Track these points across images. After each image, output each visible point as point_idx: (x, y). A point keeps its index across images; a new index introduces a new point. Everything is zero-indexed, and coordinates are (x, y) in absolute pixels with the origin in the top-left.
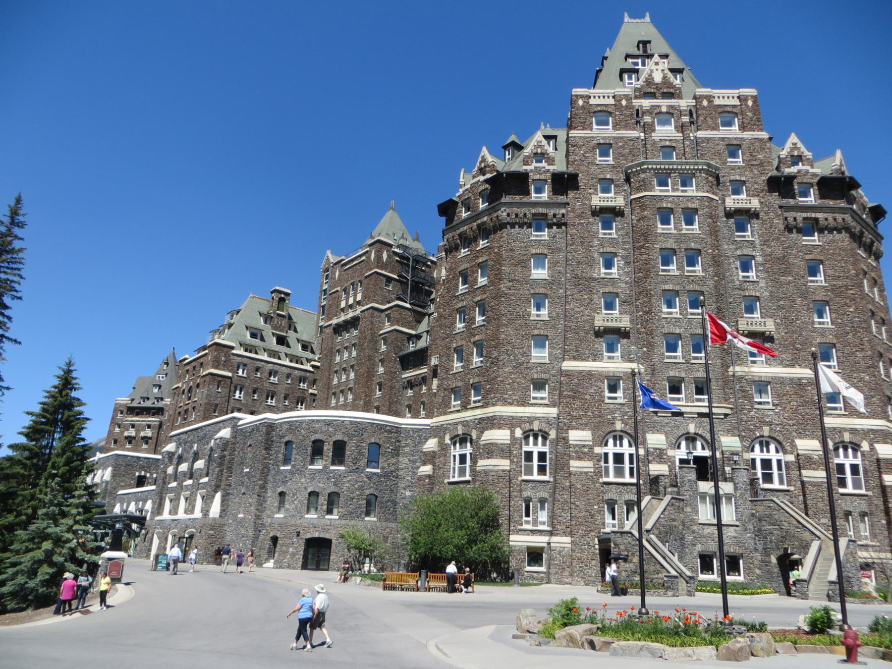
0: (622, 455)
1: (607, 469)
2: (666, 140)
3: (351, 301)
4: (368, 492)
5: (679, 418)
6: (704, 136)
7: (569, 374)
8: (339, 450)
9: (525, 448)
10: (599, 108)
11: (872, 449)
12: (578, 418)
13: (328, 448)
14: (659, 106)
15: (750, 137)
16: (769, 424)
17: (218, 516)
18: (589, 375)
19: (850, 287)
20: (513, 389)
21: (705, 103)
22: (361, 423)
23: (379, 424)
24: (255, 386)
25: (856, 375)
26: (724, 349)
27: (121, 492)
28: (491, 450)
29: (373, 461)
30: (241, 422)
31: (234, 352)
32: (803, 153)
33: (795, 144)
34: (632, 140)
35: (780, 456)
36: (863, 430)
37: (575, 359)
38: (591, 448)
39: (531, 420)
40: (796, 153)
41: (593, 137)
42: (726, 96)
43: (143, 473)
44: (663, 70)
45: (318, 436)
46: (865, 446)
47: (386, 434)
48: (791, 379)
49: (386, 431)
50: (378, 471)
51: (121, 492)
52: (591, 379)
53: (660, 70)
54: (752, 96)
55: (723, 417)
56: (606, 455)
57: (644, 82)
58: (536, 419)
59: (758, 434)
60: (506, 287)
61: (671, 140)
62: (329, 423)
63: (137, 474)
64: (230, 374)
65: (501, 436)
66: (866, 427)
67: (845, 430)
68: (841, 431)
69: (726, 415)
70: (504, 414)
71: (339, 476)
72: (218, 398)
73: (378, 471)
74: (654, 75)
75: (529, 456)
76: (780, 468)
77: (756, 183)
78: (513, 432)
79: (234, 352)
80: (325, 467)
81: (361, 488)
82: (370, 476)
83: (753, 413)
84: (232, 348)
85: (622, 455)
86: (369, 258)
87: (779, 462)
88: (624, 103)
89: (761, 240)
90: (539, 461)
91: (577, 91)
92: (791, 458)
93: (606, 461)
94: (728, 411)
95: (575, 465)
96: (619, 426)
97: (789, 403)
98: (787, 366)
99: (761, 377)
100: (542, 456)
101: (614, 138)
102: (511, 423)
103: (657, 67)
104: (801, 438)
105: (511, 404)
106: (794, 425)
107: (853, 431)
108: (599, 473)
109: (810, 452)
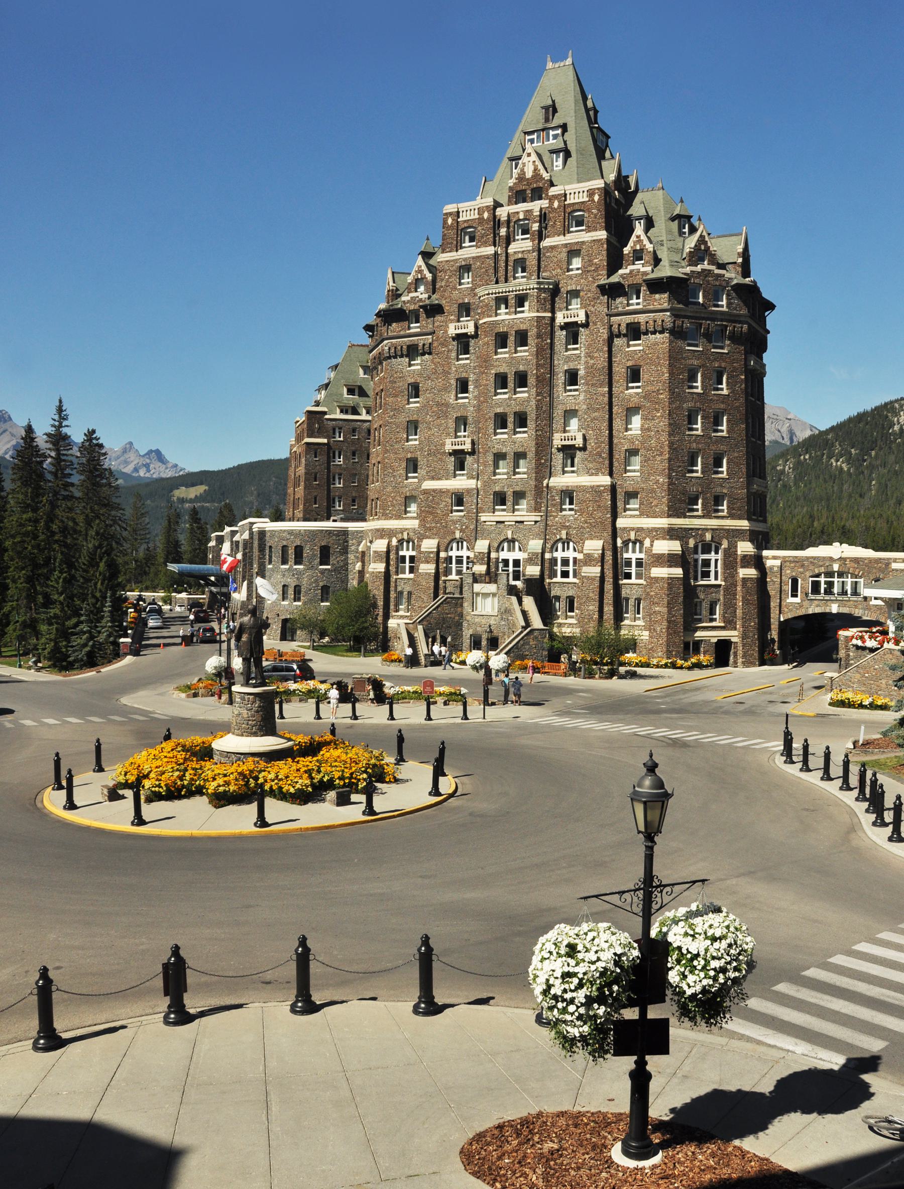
2: (519, 252)
4: (321, 584)
5: (501, 526)
6: (549, 244)
7: (426, 492)
8: (299, 551)
10: (466, 225)
11: (652, 545)
12: (430, 529)
13: (291, 551)
14: (518, 213)
15: (590, 239)
16: (568, 528)
17: (245, 599)
19: (661, 392)
20: (393, 506)
21: (556, 204)
22: (313, 531)
23: (327, 530)
24: (353, 448)
25: (652, 477)
26: (541, 464)
29: (324, 560)
30: (255, 526)
31: (327, 417)
32: (645, 245)
34: (488, 258)
35: (576, 555)
36: (648, 529)
37: (433, 478)
38: (438, 553)
39: (402, 531)
40: (638, 247)
41: (456, 260)
42: (572, 192)
44: (534, 162)
45: (285, 543)
46: (647, 542)
47: (334, 537)
48: (592, 487)
49: (334, 535)
50: (329, 567)
52: (441, 496)
53: (531, 163)
54: (598, 189)
55: (533, 523)
57: (516, 179)
59: (558, 537)
60: (389, 417)
61: (523, 251)
62: (291, 532)
64: (325, 441)
66: (650, 526)
67: (633, 529)
69: (536, 522)
70: (385, 527)
71: (300, 573)
72: (316, 466)
73: (329, 567)
74: (526, 170)
75: (404, 557)
77: (589, 291)
79: (327, 417)
80: (291, 566)
81: (316, 581)
82: (323, 572)
83: (557, 519)
84: (325, 413)
87: (575, 559)
89: (587, 353)
90: (410, 563)
91: (450, 208)
92: (580, 556)
94: (538, 519)
96: (458, 535)
97: (587, 508)
98: (592, 474)
99: (568, 487)
101: (473, 258)
103: (529, 159)
104: (592, 539)
106: (588, 527)
107: (639, 530)
109: (593, 552)
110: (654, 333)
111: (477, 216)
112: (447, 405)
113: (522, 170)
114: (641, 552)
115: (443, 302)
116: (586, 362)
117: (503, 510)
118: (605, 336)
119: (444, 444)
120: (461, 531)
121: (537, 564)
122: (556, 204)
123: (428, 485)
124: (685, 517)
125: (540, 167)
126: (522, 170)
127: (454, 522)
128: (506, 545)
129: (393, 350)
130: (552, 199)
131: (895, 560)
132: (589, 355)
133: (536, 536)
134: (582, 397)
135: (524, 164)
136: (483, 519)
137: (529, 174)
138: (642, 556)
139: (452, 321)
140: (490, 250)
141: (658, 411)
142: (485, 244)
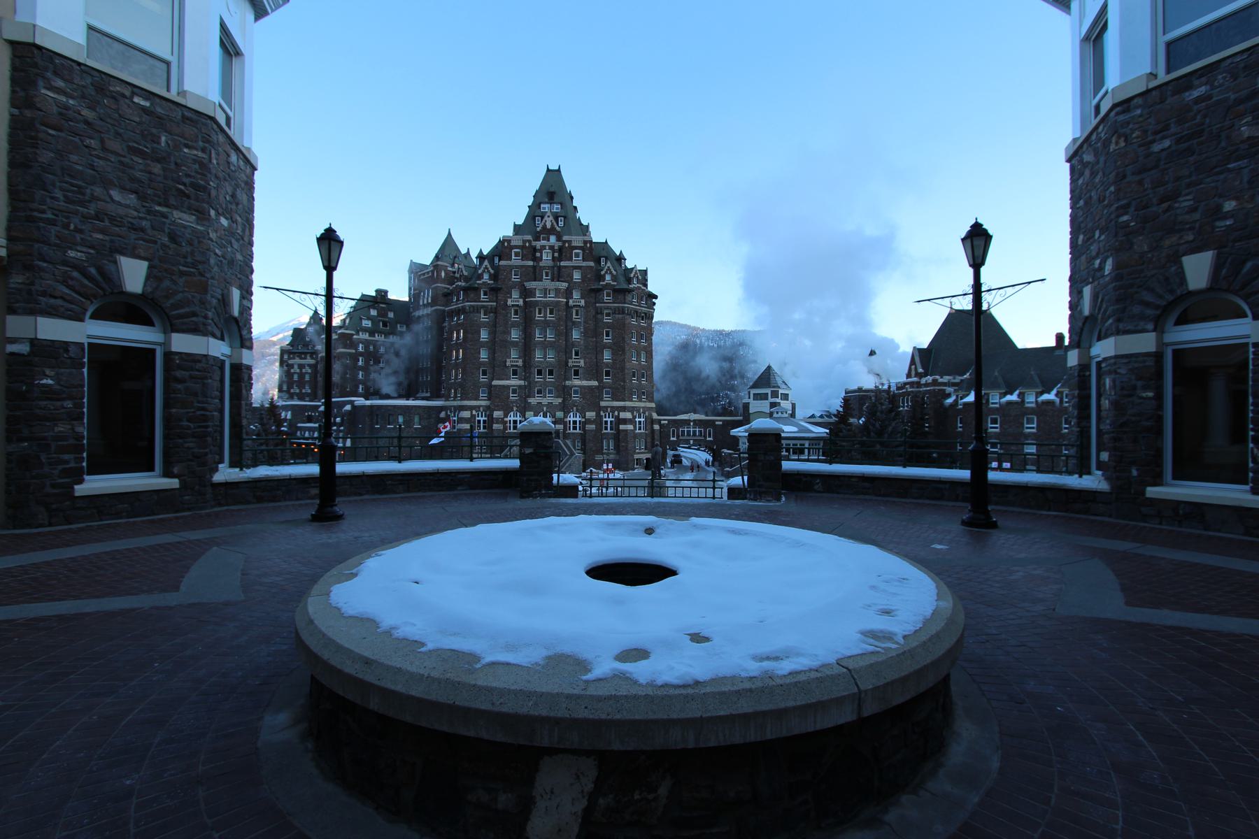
0: (516, 421)
1: (510, 427)
3: (425, 302)
9: (477, 419)
11: (619, 414)
12: (498, 406)
18: (503, 386)
21: (567, 245)
27: (299, 425)
28: (461, 420)
30: (356, 403)
31: (355, 337)
33: (608, 267)
39: (479, 407)
43: (310, 413)
46: (616, 413)
51: (299, 425)
56: (510, 421)
58: (481, 406)
63: (306, 414)
64: (354, 351)
65: (466, 414)
67: (609, 407)
68: (607, 407)
76: (580, 424)
78: (472, 412)
79: (355, 337)
85: (516, 421)
86: (433, 274)
87: (580, 421)
88: (527, 244)
92: (583, 420)
93: (510, 423)
94: (560, 401)
95: (495, 426)
100: (484, 421)
102: (470, 408)
105: (470, 400)
107: (612, 407)
108: (505, 428)
110: (619, 314)
111: (522, 244)
112: (506, 341)
113: (545, 224)
114: (612, 417)
115: (503, 286)
116: (584, 326)
117: (540, 397)
118: (594, 313)
119: (506, 361)
120: (517, 407)
121: (561, 424)
122: (567, 245)
123: (495, 383)
124: (632, 401)
125: (555, 224)
126: (545, 224)
127: (512, 402)
128: (542, 414)
129: (472, 309)
130: (565, 242)
131: (717, 421)
132: (585, 322)
133: (560, 410)
134: (582, 342)
135: (546, 221)
136: (529, 401)
137: (549, 226)
138: (613, 419)
139: (508, 297)
140: (531, 263)
141: (619, 351)
142: (527, 259)
